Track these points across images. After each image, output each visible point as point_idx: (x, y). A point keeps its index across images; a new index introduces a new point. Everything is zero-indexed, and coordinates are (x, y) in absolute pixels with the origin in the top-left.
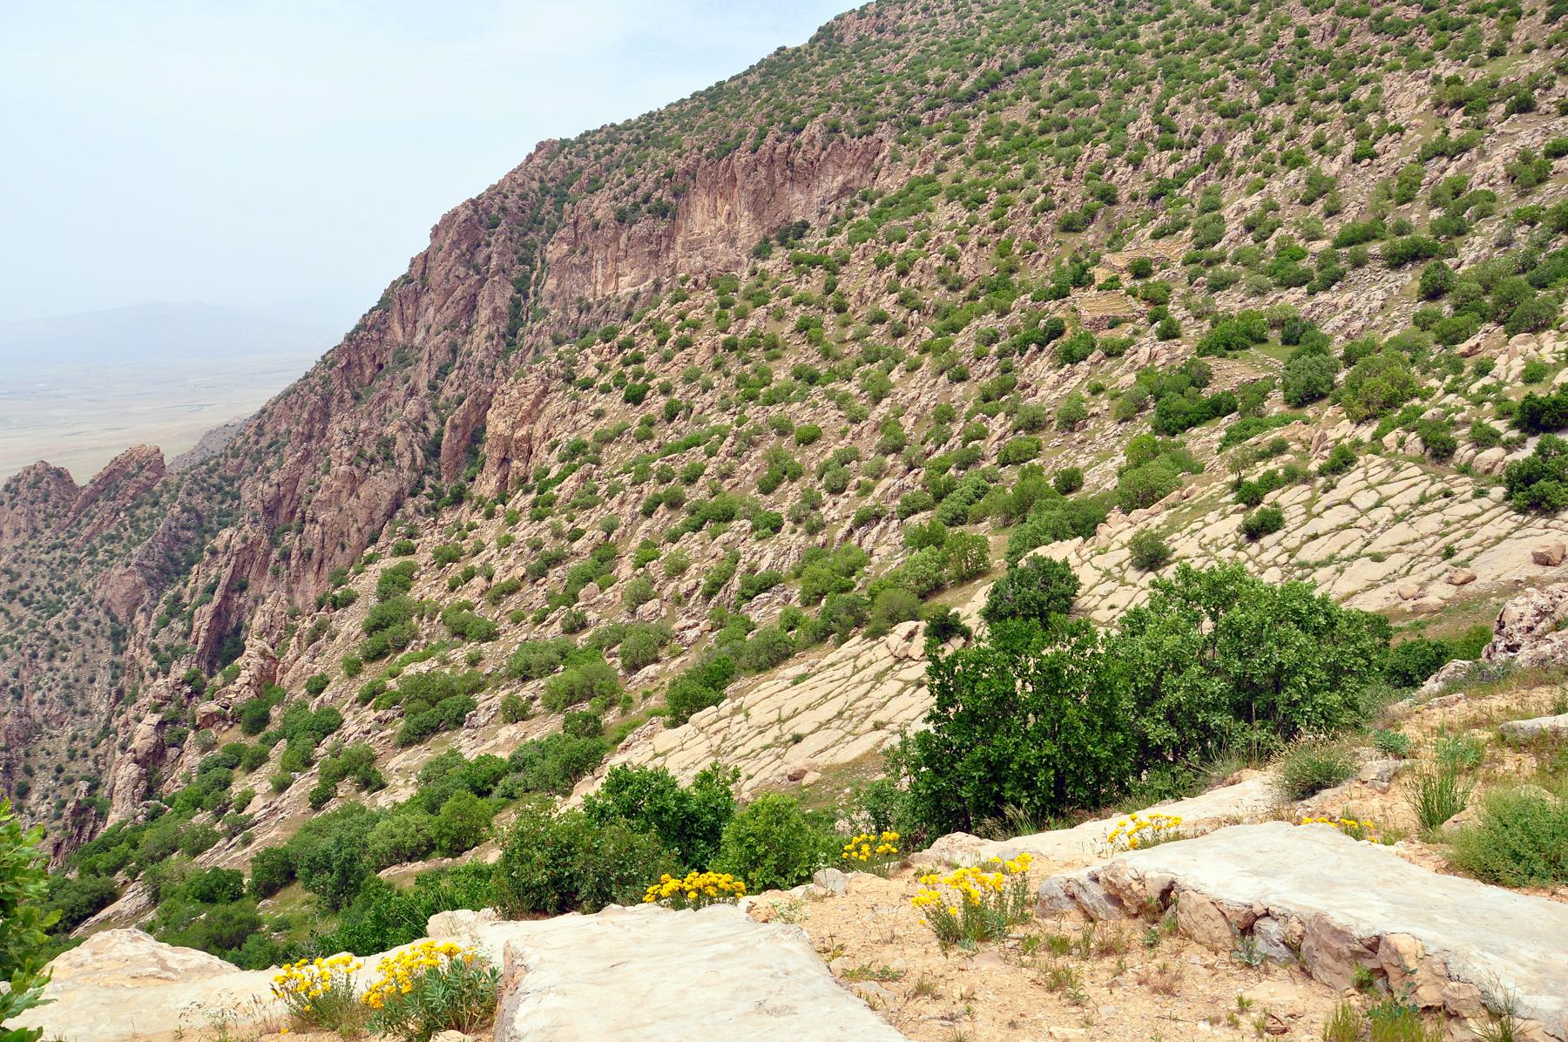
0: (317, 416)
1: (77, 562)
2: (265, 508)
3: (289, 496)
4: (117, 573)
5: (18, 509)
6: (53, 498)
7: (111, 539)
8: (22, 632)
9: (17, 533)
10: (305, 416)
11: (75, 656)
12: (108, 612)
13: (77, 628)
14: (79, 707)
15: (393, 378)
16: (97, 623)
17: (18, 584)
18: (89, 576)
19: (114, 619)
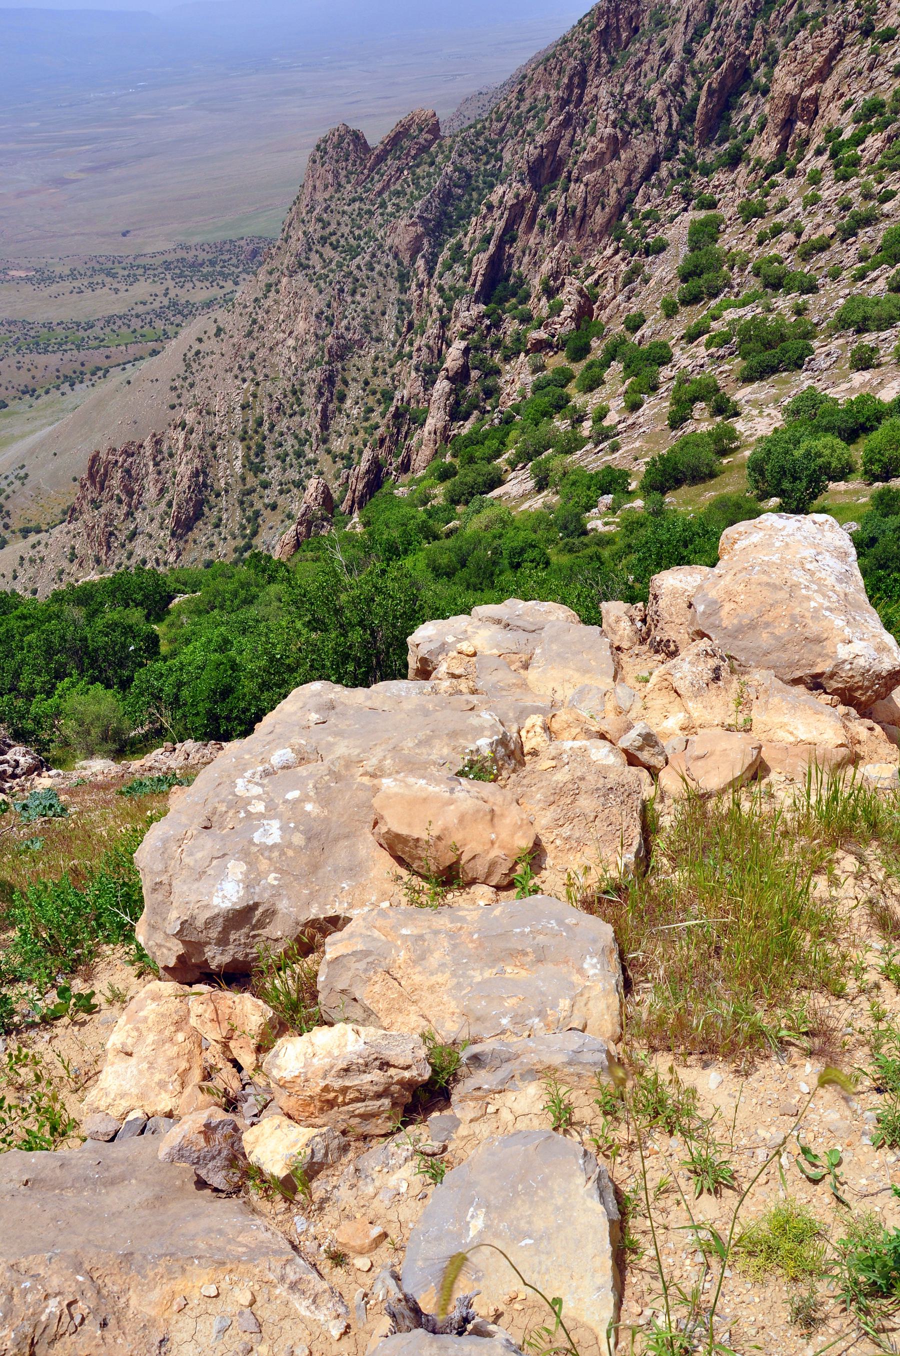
0: (576, 80)
1: (370, 213)
4: (403, 223)
5: (327, 167)
6: (352, 157)
7: (397, 194)
8: (332, 271)
9: (326, 187)
10: (566, 80)
11: (371, 292)
12: (396, 256)
13: (372, 270)
14: (374, 335)
15: (650, 42)
16: (387, 266)
17: (328, 231)
18: (381, 226)
19: (400, 263)
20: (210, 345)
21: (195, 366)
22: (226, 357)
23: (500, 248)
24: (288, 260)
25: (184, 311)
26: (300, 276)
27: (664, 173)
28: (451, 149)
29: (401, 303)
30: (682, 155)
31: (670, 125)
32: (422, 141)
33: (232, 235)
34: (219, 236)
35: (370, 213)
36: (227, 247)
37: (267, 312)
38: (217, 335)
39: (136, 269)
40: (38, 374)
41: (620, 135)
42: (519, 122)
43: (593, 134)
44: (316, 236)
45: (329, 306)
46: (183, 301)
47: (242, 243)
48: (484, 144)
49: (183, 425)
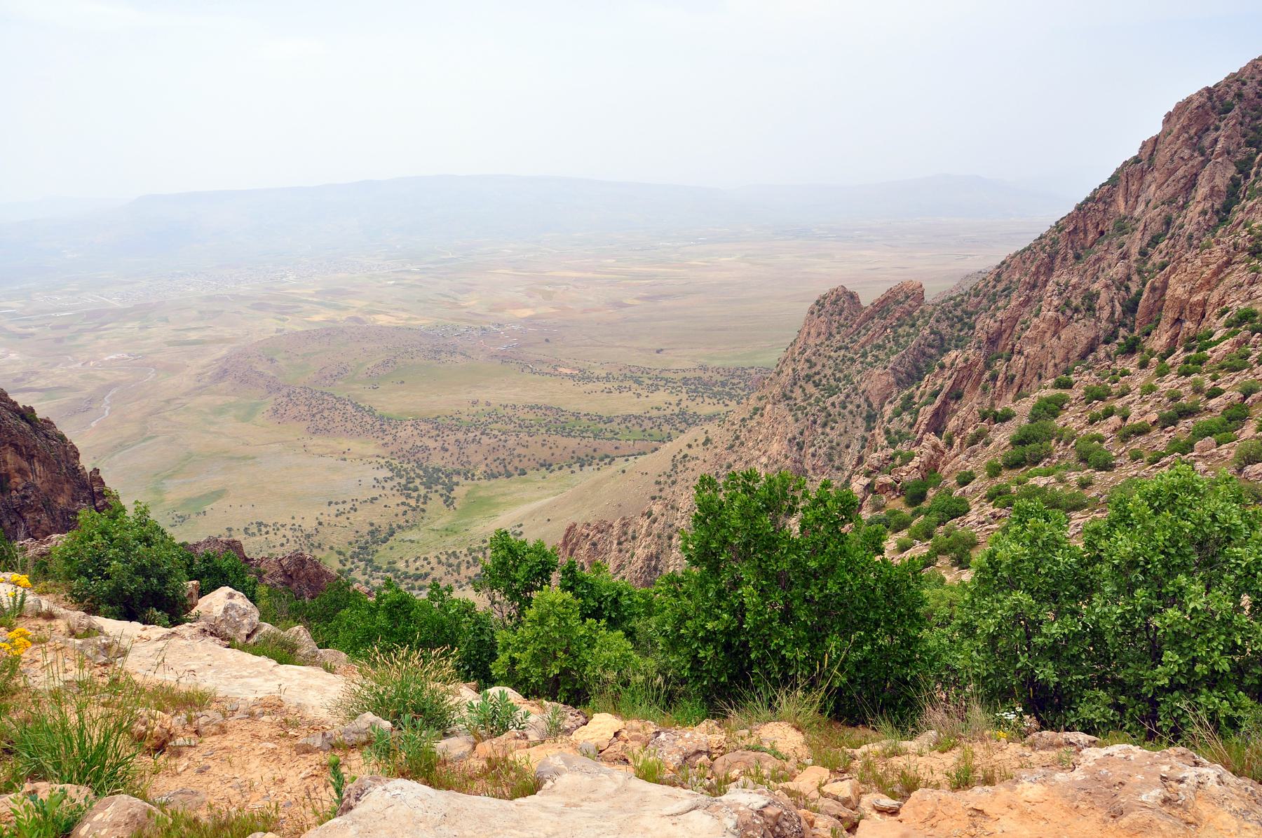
0: (1042, 270)
1: (853, 360)
2: (988, 338)
3: (1008, 331)
4: (878, 372)
5: (822, 318)
6: (845, 313)
7: (879, 347)
8: (810, 404)
9: (819, 334)
10: (1033, 269)
11: (840, 427)
12: (867, 400)
13: (845, 408)
15: (1110, 244)
16: (858, 406)
17: (813, 370)
18: (859, 372)
19: (870, 405)
20: (696, 451)
21: (680, 467)
22: (708, 464)
23: (944, 403)
24: (777, 390)
25: (687, 420)
26: (782, 405)
27: (1101, 354)
28: (931, 314)
29: (865, 439)
30: (1121, 340)
31: (1113, 313)
32: (906, 306)
33: (746, 363)
34: (733, 363)
35: (853, 360)
36: (739, 373)
37: (750, 431)
38: (705, 444)
39: (659, 381)
40: (557, 452)
41: (1061, 318)
42: (993, 299)
43: (1037, 316)
44: (803, 374)
45: (801, 433)
46: (691, 412)
47: (752, 371)
48: (959, 313)
49: (649, 514)
